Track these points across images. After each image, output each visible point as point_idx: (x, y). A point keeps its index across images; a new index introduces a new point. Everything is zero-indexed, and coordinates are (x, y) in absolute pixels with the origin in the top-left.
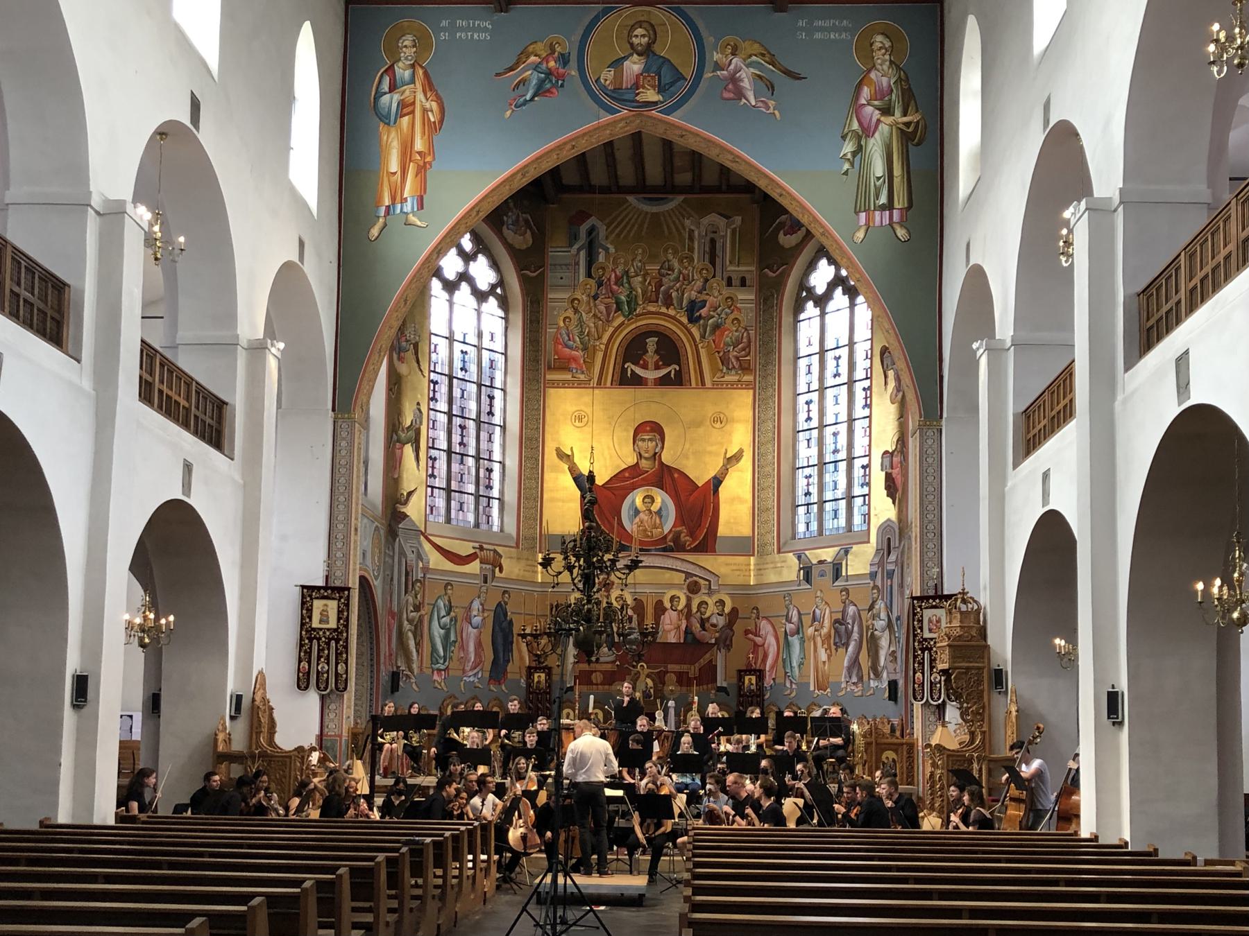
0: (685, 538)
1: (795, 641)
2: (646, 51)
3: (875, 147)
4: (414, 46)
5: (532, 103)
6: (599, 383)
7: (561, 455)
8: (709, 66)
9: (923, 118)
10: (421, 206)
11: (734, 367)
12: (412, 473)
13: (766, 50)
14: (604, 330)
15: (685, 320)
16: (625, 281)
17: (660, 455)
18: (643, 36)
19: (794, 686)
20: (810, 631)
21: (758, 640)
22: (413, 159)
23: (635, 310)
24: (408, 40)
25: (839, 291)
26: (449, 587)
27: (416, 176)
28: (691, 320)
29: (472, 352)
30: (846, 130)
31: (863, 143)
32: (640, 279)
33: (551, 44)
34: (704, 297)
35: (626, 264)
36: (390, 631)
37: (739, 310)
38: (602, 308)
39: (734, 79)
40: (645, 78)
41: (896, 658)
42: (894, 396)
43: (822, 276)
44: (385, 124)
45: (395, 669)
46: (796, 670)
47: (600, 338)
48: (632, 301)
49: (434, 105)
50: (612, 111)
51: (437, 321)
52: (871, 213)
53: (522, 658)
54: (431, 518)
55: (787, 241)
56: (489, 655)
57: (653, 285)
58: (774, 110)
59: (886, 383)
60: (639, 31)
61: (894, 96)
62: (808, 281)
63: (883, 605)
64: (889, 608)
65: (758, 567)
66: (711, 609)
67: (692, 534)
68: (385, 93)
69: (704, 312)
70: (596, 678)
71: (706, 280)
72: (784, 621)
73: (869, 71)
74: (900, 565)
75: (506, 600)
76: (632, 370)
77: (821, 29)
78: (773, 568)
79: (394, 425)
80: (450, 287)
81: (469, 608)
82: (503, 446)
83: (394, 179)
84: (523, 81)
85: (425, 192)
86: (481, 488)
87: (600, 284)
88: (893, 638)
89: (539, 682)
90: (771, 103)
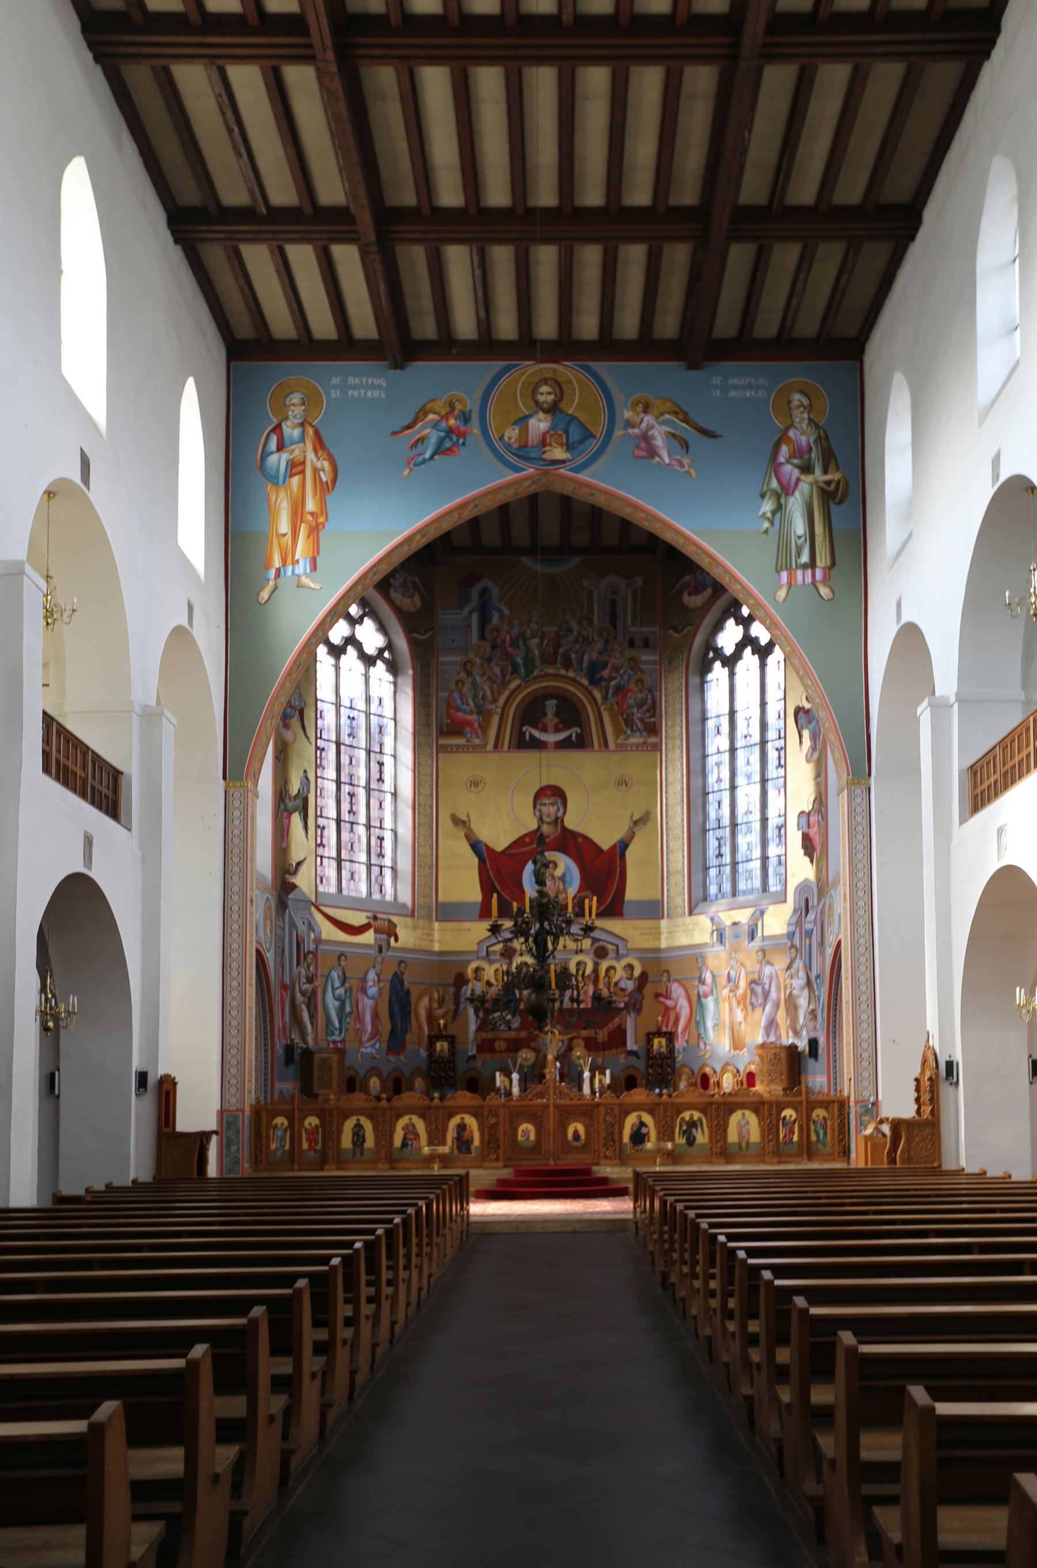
2: (553, 409)
3: (795, 506)
4: (303, 404)
5: (432, 462)
6: (496, 746)
7: (456, 821)
8: (619, 424)
9: (844, 477)
10: (314, 567)
11: (638, 729)
12: (300, 844)
13: (679, 407)
14: (500, 693)
16: (521, 642)
18: (549, 393)
21: (670, 1003)
22: (304, 519)
23: (532, 672)
24: (296, 398)
25: (748, 650)
26: (343, 958)
27: (308, 537)
28: (592, 682)
29: (362, 718)
30: (765, 488)
31: (782, 501)
32: (536, 641)
33: (451, 401)
36: (283, 1003)
37: (643, 672)
38: (497, 670)
39: (646, 437)
40: (552, 436)
41: (816, 1017)
42: (809, 755)
43: (729, 636)
44: (273, 484)
45: (289, 1042)
47: (495, 701)
48: (529, 664)
49: (326, 465)
50: (517, 469)
51: (324, 689)
52: (793, 572)
53: (420, 1028)
54: (321, 889)
55: (693, 601)
56: (386, 1026)
58: (689, 467)
59: (801, 742)
60: (545, 389)
61: (813, 455)
62: (715, 641)
63: (801, 965)
64: (808, 967)
66: (619, 974)
68: (272, 453)
69: (605, 673)
70: (500, 1045)
71: (607, 642)
72: (696, 983)
73: (787, 429)
74: (819, 924)
75: (402, 969)
76: (531, 735)
77: (737, 387)
79: (281, 794)
80: (337, 651)
81: (364, 980)
82: (395, 814)
83: (284, 540)
84: (422, 440)
85: (318, 553)
86: (373, 856)
87: (494, 647)
88: (812, 996)
89: (442, 1051)
90: (686, 461)
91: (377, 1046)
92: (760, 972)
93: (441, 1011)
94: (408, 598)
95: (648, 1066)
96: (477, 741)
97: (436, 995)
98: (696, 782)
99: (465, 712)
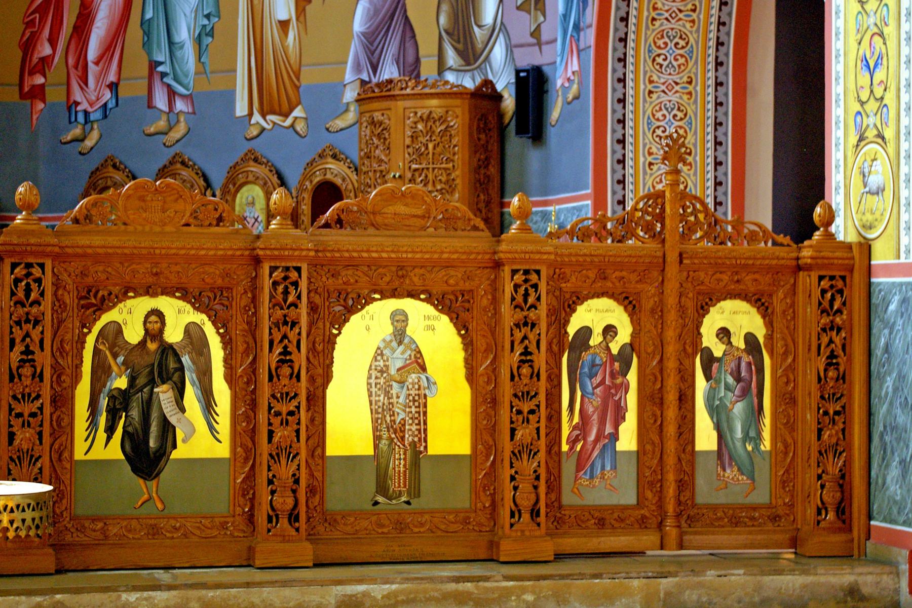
46: (189, 54)
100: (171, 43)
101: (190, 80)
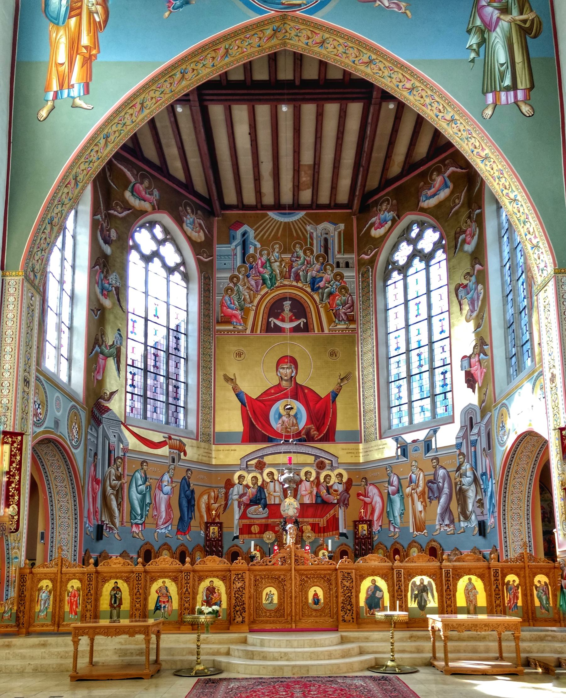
0: (314, 432)
1: (396, 499)
6: (252, 331)
7: (227, 379)
11: (343, 320)
14: (255, 297)
15: (309, 290)
16: (268, 265)
17: (295, 378)
19: (397, 530)
20: (408, 490)
23: (275, 284)
28: (313, 290)
32: (278, 264)
34: (321, 275)
35: (268, 254)
37: (345, 282)
38: (253, 283)
47: (252, 302)
48: (273, 278)
53: (202, 517)
57: (287, 267)
65: (366, 450)
67: (318, 429)
69: (321, 284)
72: (387, 485)
75: (189, 475)
76: (274, 322)
78: (376, 450)
82: (186, 372)
89: (213, 533)
91: (170, 528)
92: (435, 474)
93: (216, 505)
94: (196, 232)
95: (355, 544)
96: (240, 328)
97: (213, 494)
98: (382, 350)
99: (233, 309)
100: (394, 516)
101: (399, 524)
